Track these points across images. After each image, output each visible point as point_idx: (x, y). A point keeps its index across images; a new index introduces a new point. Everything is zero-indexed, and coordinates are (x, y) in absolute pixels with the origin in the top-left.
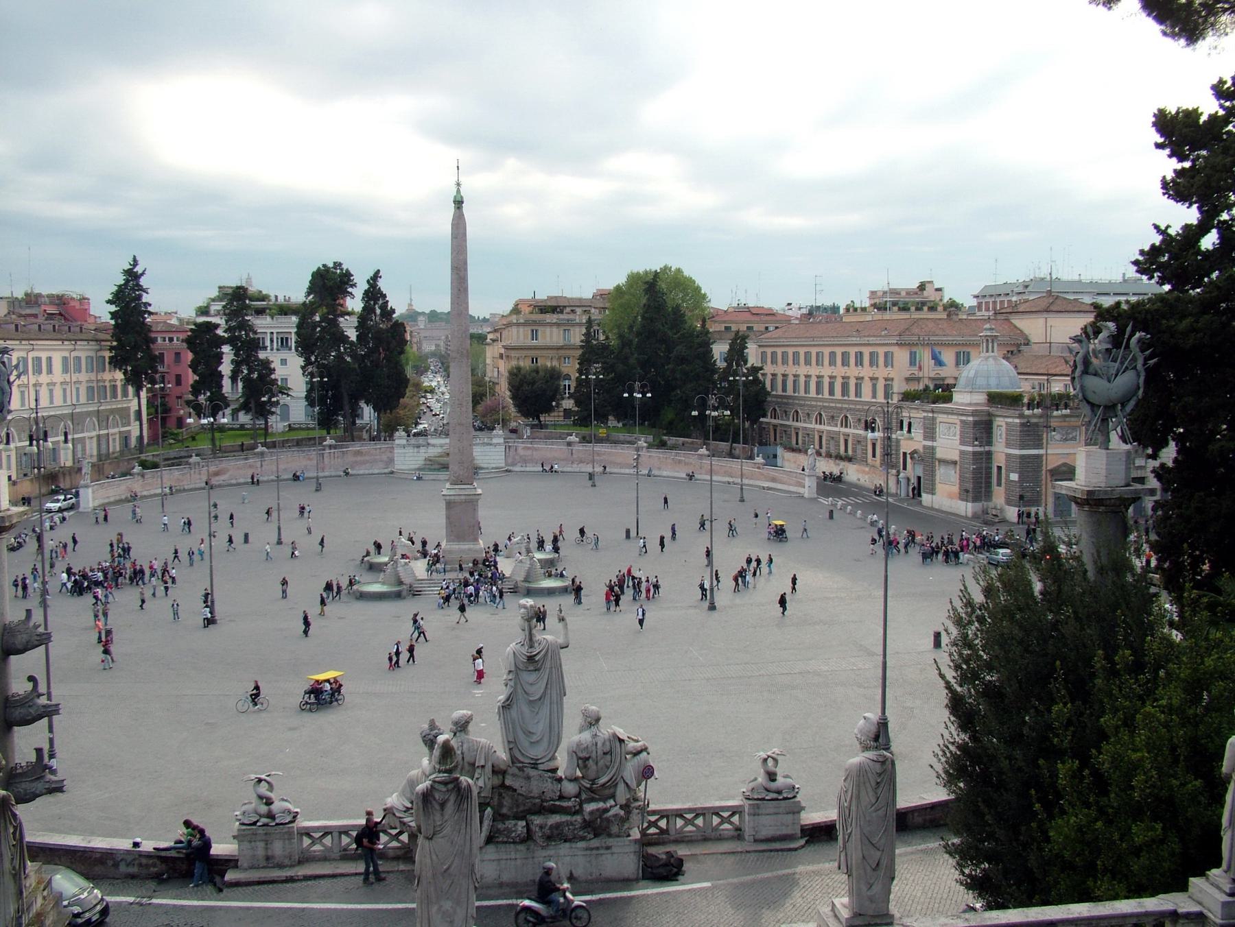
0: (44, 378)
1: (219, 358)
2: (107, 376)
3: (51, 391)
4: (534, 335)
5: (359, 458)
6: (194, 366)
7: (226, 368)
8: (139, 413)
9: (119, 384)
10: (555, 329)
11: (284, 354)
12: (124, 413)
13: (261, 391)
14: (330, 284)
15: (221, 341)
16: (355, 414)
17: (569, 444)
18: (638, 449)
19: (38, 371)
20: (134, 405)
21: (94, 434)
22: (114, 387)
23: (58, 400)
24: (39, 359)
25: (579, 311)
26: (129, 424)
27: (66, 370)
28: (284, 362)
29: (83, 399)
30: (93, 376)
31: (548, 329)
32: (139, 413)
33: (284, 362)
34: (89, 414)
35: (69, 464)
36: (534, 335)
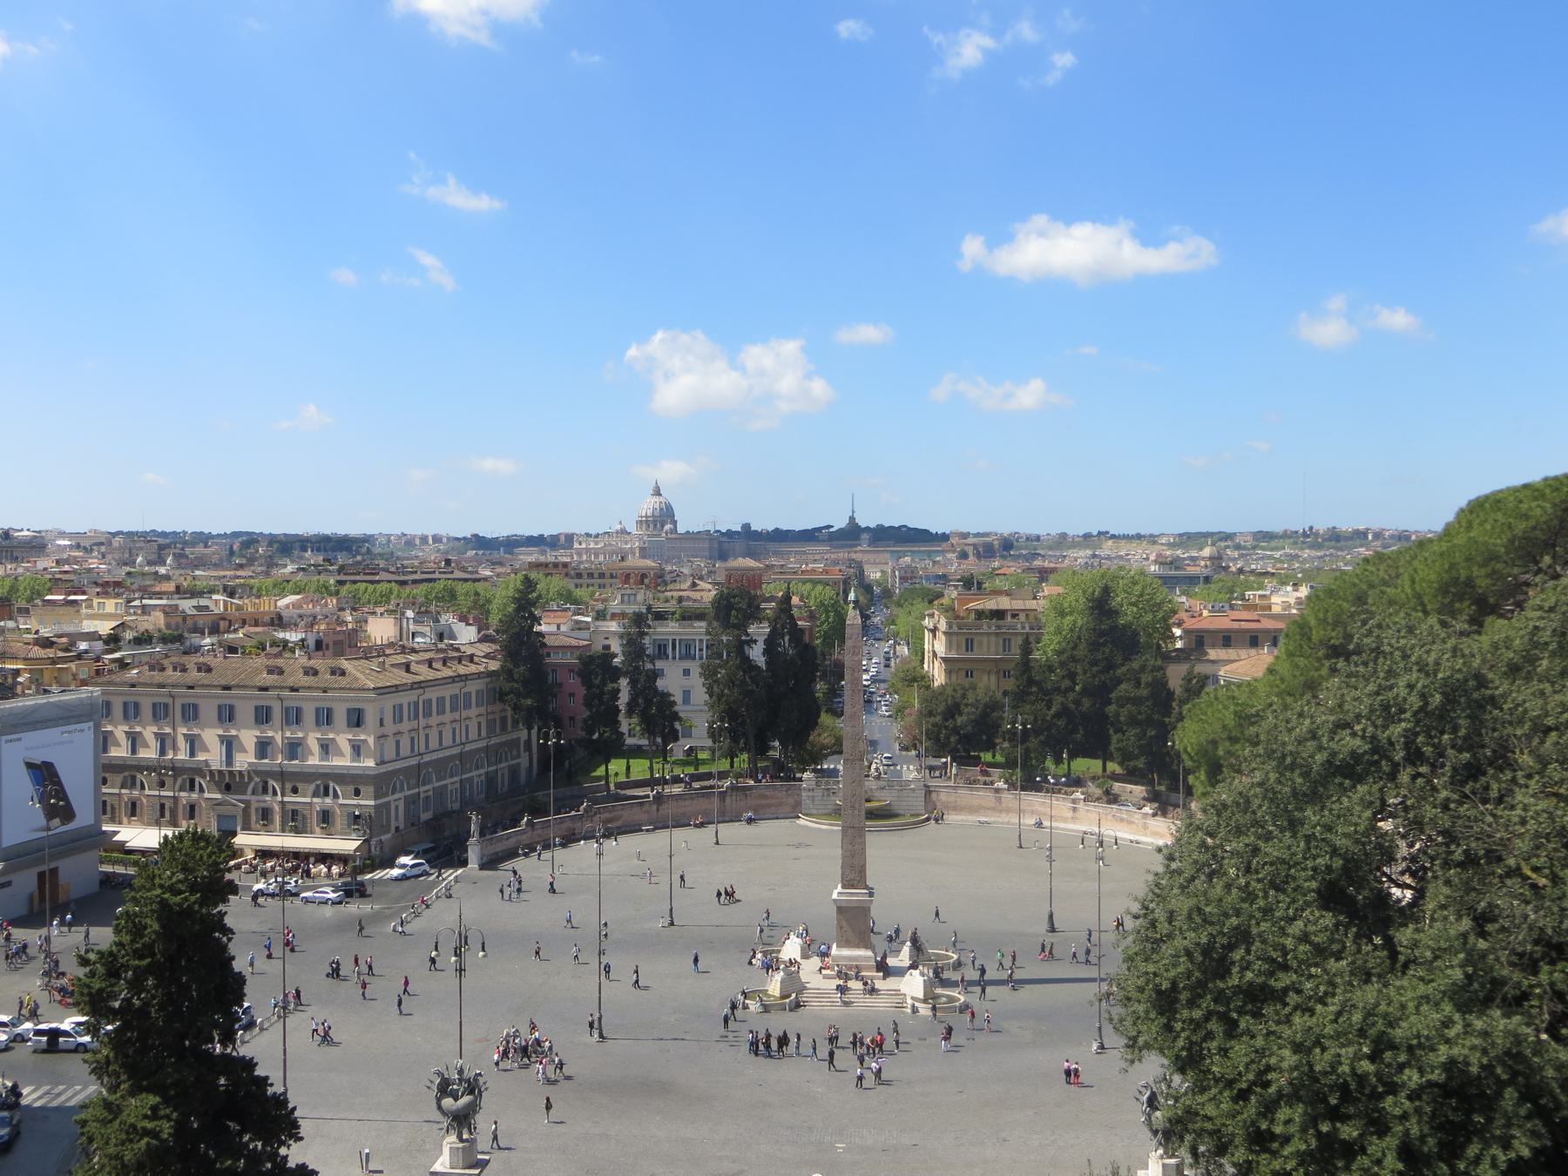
0: (434, 720)
1: (615, 693)
2: (498, 706)
3: (441, 733)
4: (969, 645)
5: (763, 802)
6: (588, 703)
7: (624, 698)
8: (528, 742)
9: (509, 713)
10: (993, 639)
11: (687, 664)
12: (514, 743)
13: (661, 719)
14: (736, 606)
15: (615, 674)
16: (761, 749)
17: (997, 791)
18: (1074, 801)
19: (428, 714)
20: (523, 735)
21: (482, 771)
22: (504, 720)
23: (447, 741)
24: (430, 701)
25: (1022, 617)
26: (518, 756)
27: (453, 710)
28: (686, 672)
29: (473, 735)
30: (482, 710)
31: (985, 639)
32: (528, 742)
33: (686, 672)
34: (479, 750)
35: (456, 806)
36: (969, 645)
